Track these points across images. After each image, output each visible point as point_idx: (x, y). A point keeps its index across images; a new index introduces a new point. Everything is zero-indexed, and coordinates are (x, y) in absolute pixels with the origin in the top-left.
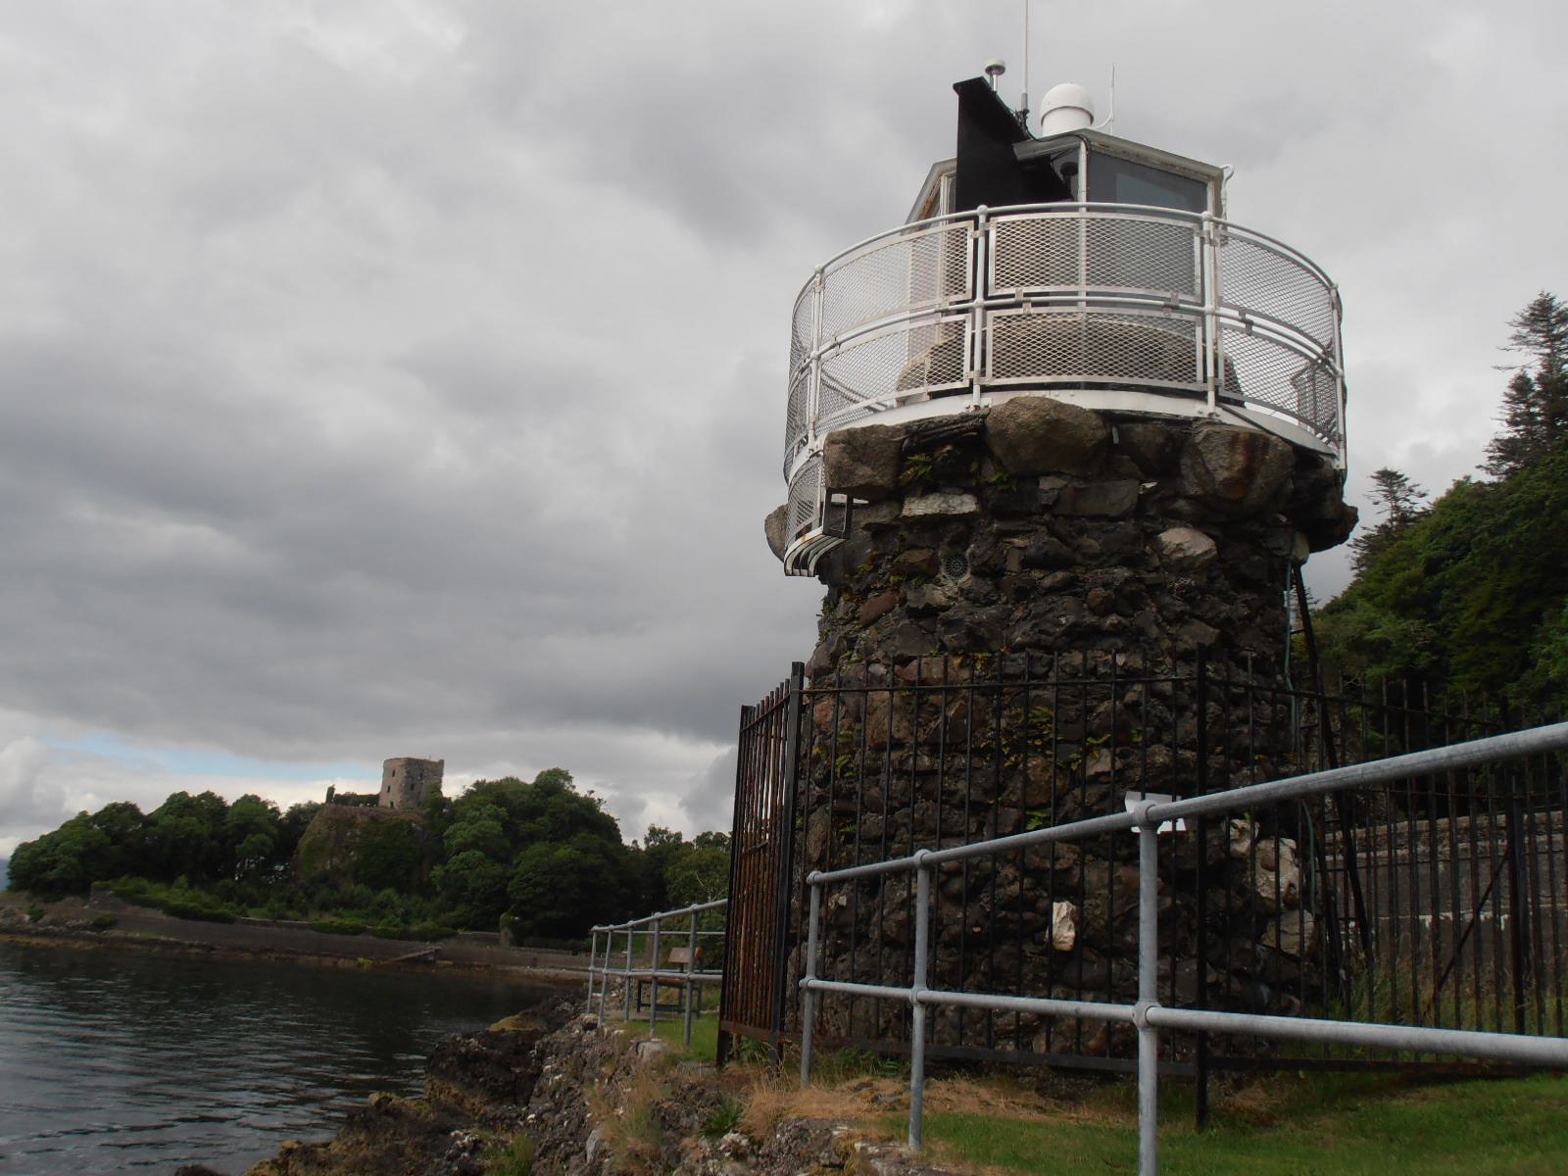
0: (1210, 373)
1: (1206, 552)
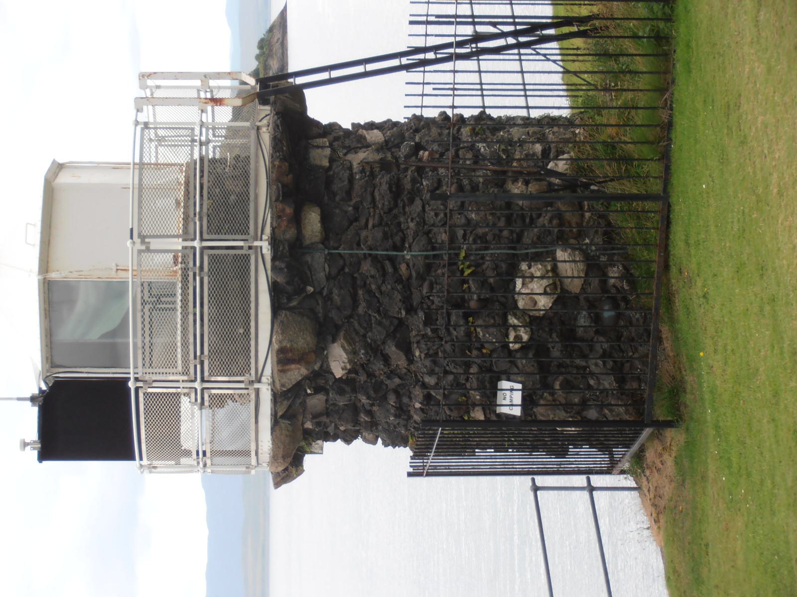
0: (242, 385)
1: (343, 347)
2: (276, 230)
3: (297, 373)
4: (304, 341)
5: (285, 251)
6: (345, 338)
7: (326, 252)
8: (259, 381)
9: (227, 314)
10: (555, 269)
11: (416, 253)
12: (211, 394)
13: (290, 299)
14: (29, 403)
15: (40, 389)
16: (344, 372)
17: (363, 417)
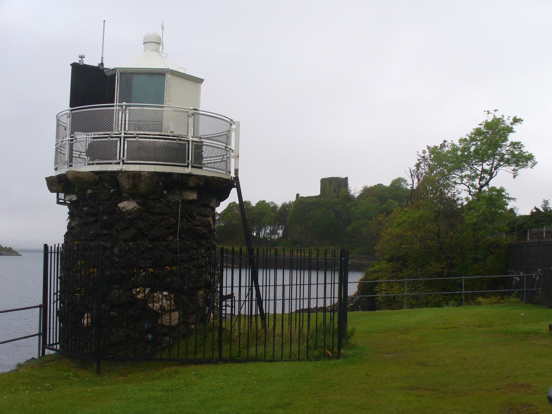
1: (134, 208)
2: (194, 177)
3: (125, 184)
4: (143, 188)
5: (185, 181)
6: (138, 208)
7: (180, 201)
8: (124, 163)
9: (152, 151)
10: (171, 311)
11: (178, 244)
12: (117, 141)
13: (162, 181)
14: (100, 63)
15: (106, 69)
16: (121, 208)
17: (92, 219)
